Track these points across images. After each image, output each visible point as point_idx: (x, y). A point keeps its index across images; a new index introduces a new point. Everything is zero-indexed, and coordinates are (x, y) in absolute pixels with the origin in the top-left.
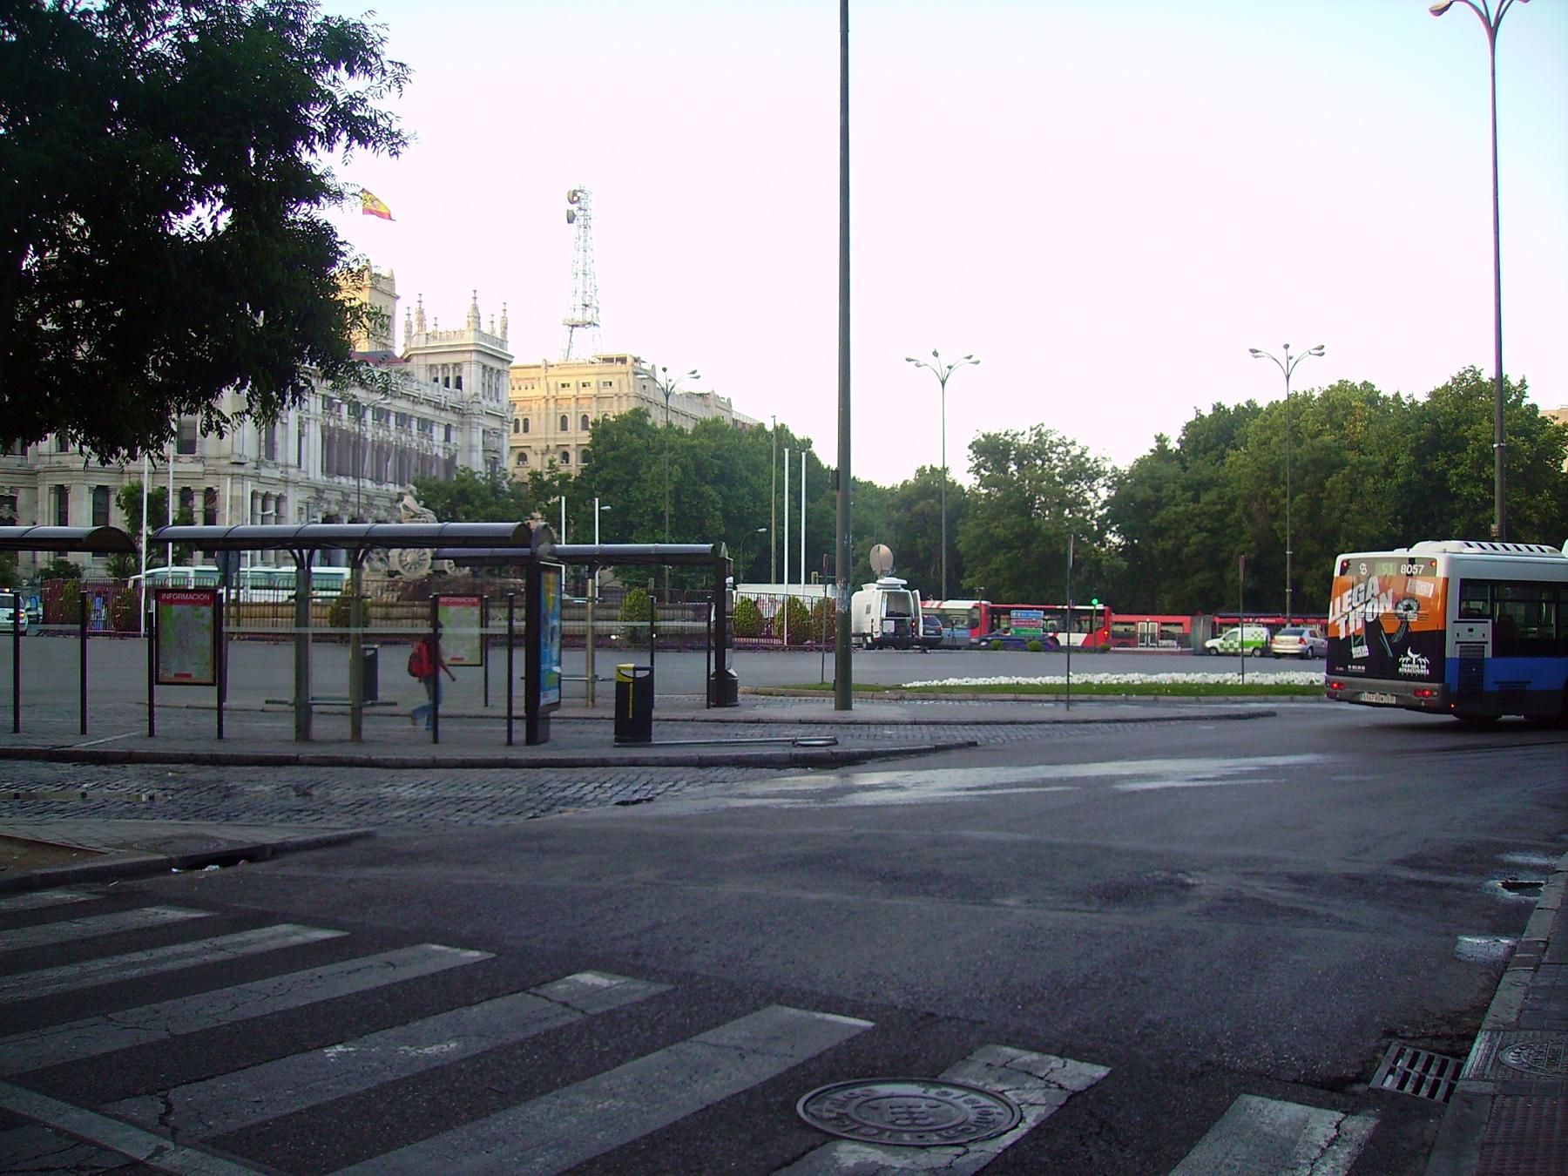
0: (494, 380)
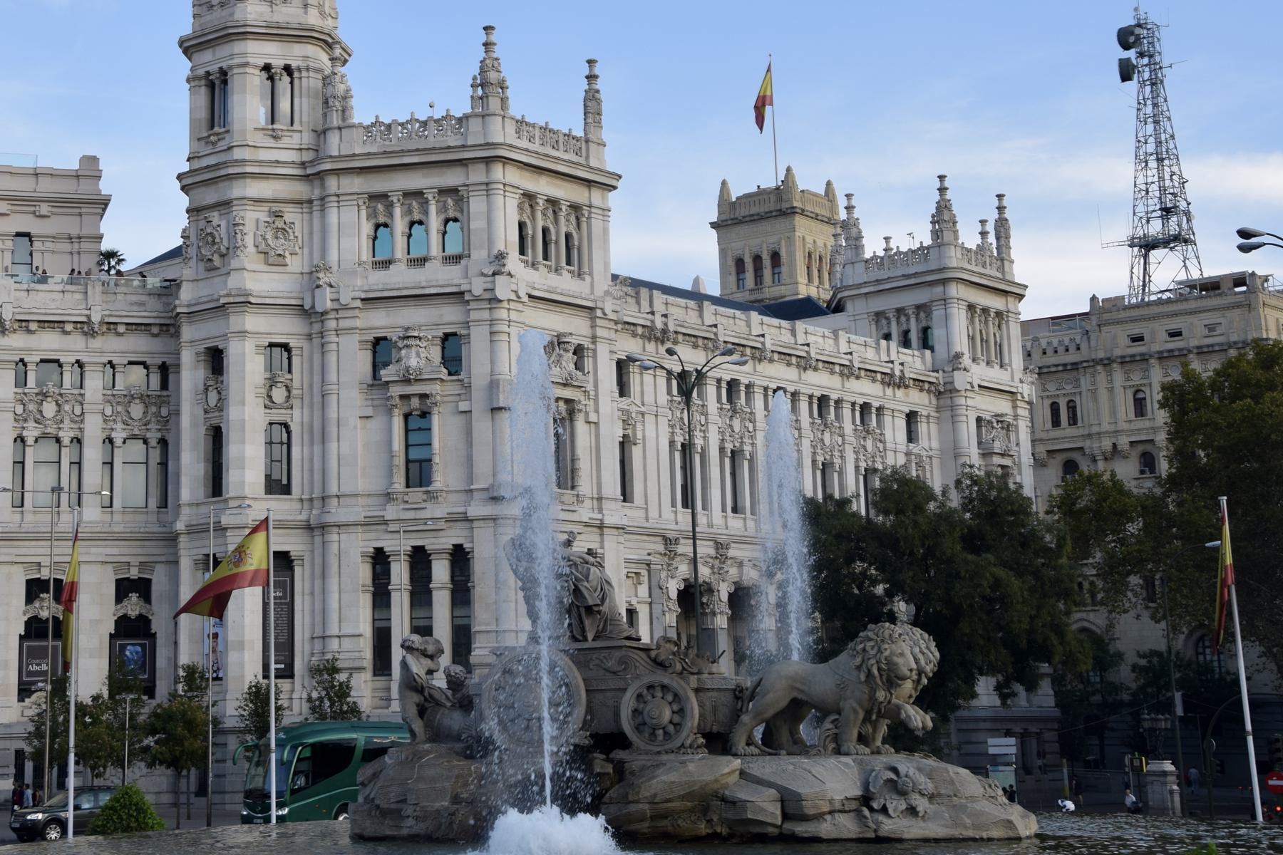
0: (992, 330)
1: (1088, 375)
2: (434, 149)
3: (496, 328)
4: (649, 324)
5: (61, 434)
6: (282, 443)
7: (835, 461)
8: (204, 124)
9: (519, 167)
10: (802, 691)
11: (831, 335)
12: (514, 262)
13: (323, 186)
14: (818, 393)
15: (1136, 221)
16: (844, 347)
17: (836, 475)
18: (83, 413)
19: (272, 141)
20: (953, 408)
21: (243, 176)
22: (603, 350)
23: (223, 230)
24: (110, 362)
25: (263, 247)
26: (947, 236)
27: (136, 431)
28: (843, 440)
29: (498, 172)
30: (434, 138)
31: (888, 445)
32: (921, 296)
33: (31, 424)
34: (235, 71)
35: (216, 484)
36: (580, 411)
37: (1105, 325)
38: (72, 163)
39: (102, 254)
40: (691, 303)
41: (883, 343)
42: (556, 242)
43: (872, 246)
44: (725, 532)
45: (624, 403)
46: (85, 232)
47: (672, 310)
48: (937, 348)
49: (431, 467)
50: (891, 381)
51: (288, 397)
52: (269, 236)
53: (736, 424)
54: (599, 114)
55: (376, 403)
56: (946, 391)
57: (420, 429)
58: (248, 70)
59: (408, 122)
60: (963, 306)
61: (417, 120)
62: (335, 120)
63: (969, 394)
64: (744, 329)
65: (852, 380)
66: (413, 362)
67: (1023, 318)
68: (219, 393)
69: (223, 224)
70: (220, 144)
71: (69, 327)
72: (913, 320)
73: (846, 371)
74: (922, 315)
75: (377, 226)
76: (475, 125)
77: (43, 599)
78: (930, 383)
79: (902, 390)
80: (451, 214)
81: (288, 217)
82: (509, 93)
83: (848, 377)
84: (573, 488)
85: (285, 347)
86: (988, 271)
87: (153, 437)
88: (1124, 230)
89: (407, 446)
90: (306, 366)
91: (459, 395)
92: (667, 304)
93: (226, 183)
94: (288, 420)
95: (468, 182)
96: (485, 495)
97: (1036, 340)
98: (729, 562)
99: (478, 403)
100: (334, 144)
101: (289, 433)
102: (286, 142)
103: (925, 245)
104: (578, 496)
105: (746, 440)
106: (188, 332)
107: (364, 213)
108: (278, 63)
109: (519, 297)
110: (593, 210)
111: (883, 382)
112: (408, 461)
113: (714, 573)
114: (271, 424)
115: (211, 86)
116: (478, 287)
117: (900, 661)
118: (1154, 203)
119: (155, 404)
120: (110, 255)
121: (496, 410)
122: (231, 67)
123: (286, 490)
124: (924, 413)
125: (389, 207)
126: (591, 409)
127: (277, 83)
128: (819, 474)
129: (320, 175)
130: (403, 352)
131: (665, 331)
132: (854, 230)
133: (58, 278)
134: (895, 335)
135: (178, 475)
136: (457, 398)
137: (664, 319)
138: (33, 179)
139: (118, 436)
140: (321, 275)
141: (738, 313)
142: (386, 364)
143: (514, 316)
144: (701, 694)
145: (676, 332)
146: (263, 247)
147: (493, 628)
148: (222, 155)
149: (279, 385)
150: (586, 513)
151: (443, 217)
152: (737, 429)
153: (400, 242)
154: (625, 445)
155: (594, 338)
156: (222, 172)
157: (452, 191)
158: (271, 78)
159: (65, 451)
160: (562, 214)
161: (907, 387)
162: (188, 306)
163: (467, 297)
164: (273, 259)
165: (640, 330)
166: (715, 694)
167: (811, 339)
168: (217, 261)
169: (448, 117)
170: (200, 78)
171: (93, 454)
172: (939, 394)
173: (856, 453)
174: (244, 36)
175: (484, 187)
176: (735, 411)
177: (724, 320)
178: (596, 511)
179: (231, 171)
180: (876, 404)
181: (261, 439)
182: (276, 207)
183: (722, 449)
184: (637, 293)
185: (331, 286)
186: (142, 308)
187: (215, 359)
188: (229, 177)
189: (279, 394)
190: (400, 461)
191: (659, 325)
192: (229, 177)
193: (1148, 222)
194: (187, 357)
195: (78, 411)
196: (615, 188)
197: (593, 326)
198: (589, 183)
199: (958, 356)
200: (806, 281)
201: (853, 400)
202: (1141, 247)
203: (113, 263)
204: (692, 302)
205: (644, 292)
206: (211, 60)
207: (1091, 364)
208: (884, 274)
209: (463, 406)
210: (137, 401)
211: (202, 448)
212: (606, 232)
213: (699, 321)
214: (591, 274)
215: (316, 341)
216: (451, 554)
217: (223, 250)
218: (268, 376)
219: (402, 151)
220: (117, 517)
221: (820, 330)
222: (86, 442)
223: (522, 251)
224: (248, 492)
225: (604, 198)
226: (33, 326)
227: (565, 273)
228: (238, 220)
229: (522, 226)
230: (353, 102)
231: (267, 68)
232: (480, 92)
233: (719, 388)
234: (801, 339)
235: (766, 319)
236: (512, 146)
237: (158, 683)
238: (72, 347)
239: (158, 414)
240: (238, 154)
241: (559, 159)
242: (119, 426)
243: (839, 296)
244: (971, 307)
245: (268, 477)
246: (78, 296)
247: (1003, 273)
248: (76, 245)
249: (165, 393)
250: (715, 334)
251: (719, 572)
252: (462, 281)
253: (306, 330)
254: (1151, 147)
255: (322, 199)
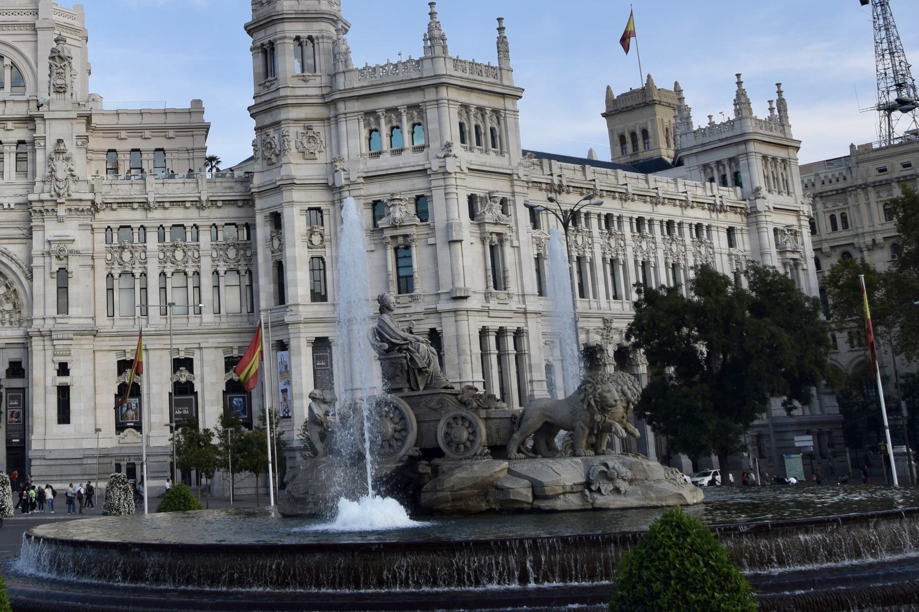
0: (780, 170)
1: (853, 196)
2: (402, 81)
3: (448, 191)
4: (549, 182)
5: (187, 270)
6: (320, 270)
7: (680, 262)
8: (262, 76)
9: (457, 89)
10: (551, 417)
11: (673, 181)
12: (457, 148)
13: (336, 109)
14: (666, 219)
15: (880, 94)
16: (681, 188)
17: (682, 271)
18: (199, 256)
19: (303, 83)
20: (757, 223)
21: (287, 105)
22: (520, 201)
23: (276, 140)
24: (214, 225)
25: (301, 149)
26: (745, 113)
27: (232, 266)
28: (685, 248)
29: (443, 92)
30: (402, 75)
31: (715, 250)
32: (731, 153)
33: (169, 264)
34: (278, 42)
35: (281, 296)
36: (507, 240)
37: (861, 162)
38: (187, 106)
39: (207, 159)
40: (578, 166)
41: (708, 184)
42: (485, 134)
43: (699, 121)
44: (609, 312)
45: (536, 233)
46: (197, 145)
47: (565, 172)
48: (744, 185)
49: (413, 280)
50: (714, 208)
51: (322, 241)
52: (305, 141)
53: (613, 242)
54: (507, 51)
55: (376, 242)
56: (752, 212)
57: (405, 257)
58: (286, 41)
59: (385, 66)
60: (759, 157)
61: (391, 64)
62: (341, 68)
63: (767, 213)
64: (615, 182)
65: (689, 209)
66: (398, 215)
67: (801, 162)
68: (280, 240)
69: (276, 136)
70: (272, 87)
71: (188, 205)
72: (727, 168)
73: (684, 204)
74: (733, 164)
75: (371, 132)
76: (427, 64)
77: (181, 371)
78: (741, 208)
79: (723, 214)
80: (416, 120)
81: (316, 129)
82: (447, 42)
83: (685, 208)
84: (505, 289)
85: (319, 210)
86: (774, 133)
87: (243, 269)
88: (874, 102)
89: (398, 268)
90: (332, 221)
91: (428, 234)
92: (561, 168)
93: (277, 111)
94: (323, 255)
95: (425, 100)
96: (447, 296)
97: (817, 175)
98: (613, 331)
99: (440, 238)
100: (341, 83)
101: (324, 263)
102: (312, 83)
103: (731, 119)
104: (508, 294)
105: (620, 252)
106: (259, 204)
107: (362, 124)
108: (304, 35)
109: (462, 170)
110: (507, 112)
111: (709, 209)
112: (399, 277)
113: (603, 339)
114: (312, 258)
115: (265, 52)
116: (435, 165)
117: (608, 395)
118: (891, 82)
119: (243, 249)
120: (212, 159)
121: (452, 242)
122: (275, 40)
123: (324, 298)
124: (739, 227)
125: (378, 119)
126: (514, 238)
127: (305, 47)
128: (670, 271)
129: (334, 102)
130: (391, 209)
131: (560, 186)
132: (685, 113)
133: (181, 175)
134: (717, 179)
135: (258, 292)
136: (426, 236)
137: (559, 178)
138: (164, 116)
139: (222, 269)
140: (337, 164)
141: (609, 171)
142: (381, 217)
143: (459, 182)
144: (489, 421)
145: (568, 186)
146: (301, 149)
147: (458, 380)
148: (274, 93)
149: (316, 233)
150: (514, 304)
151: (411, 123)
152: (613, 245)
153: (386, 140)
154: (539, 259)
155: (513, 193)
156: (274, 104)
157: (415, 106)
158: (301, 45)
159: (190, 280)
160: (487, 116)
161: (726, 211)
162: (258, 188)
163: (429, 172)
164: (308, 156)
165: (544, 186)
166: (497, 421)
167: (659, 185)
168: (274, 159)
169: (410, 61)
170: (258, 48)
171: (207, 281)
172: (748, 215)
173: (695, 256)
174: (282, 20)
175: (435, 103)
176: (611, 234)
177: (600, 176)
178: (521, 303)
179: (279, 103)
180: (705, 224)
181: (307, 267)
182: (308, 124)
183: (604, 259)
184: (541, 163)
185: (344, 170)
186: (232, 191)
187: (276, 220)
188: (278, 107)
189: (316, 239)
190: (393, 277)
191: (556, 182)
192: (278, 107)
193: (888, 93)
194: (259, 219)
195: (196, 255)
196: (520, 97)
197: (512, 186)
198: (503, 95)
199: (758, 189)
200: (666, 147)
201: (690, 222)
202: (885, 110)
203: (214, 164)
204: (578, 166)
205: (545, 162)
206: (264, 36)
207: (854, 188)
208: (706, 140)
209: (431, 241)
210: (232, 248)
211: (271, 274)
212: (516, 125)
213: (583, 178)
214: (508, 153)
215: (337, 205)
216: (429, 335)
217: (277, 152)
218: (309, 228)
219: (383, 84)
220: (223, 319)
221: (665, 179)
222: (202, 274)
223: (463, 141)
224: (300, 301)
225: (514, 104)
226: (167, 205)
227: (491, 153)
228: (285, 133)
229: (461, 125)
230: (352, 56)
231: (298, 38)
232: (429, 43)
233: (599, 220)
234: (652, 185)
235: (629, 174)
236: (451, 76)
237: (254, 420)
238: (190, 216)
239: (245, 255)
240: (282, 93)
241: (482, 81)
242: (222, 263)
243: (679, 155)
244: (765, 157)
245: (312, 291)
246: (193, 185)
247: (784, 133)
248: (191, 154)
249: (248, 242)
250: (594, 186)
251: (607, 338)
252: (425, 162)
253: (331, 199)
254: (885, 46)
255: (336, 116)
